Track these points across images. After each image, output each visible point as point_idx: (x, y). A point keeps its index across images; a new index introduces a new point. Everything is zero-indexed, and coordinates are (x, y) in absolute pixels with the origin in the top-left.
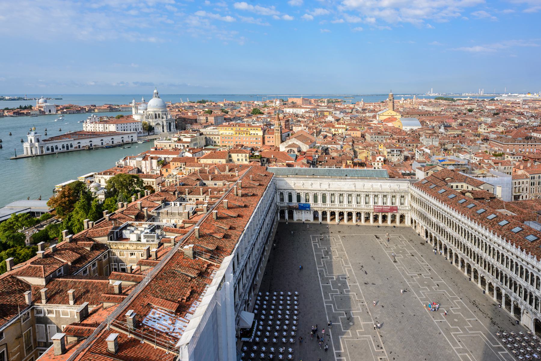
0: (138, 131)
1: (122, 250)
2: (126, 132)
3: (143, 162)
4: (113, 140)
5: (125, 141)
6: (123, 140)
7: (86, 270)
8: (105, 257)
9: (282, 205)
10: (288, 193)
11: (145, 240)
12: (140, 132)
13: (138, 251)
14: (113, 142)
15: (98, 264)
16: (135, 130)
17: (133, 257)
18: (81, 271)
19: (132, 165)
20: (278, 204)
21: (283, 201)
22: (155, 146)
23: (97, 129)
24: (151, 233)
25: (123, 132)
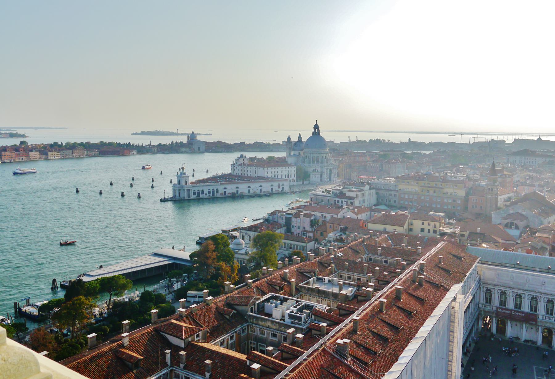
0: (291, 179)
1: (262, 327)
4: (261, 188)
5: (274, 190)
6: (272, 189)
7: (224, 341)
8: (243, 330)
9: (487, 309)
10: (499, 292)
11: (290, 321)
12: (293, 179)
13: (281, 332)
14: (261, 190)
15: (236, 338)
17: (273, 339)
18: (218, 342)
20: (480, 306)
21: (490, 303)
23: (245, 173)
24: (298, 313)
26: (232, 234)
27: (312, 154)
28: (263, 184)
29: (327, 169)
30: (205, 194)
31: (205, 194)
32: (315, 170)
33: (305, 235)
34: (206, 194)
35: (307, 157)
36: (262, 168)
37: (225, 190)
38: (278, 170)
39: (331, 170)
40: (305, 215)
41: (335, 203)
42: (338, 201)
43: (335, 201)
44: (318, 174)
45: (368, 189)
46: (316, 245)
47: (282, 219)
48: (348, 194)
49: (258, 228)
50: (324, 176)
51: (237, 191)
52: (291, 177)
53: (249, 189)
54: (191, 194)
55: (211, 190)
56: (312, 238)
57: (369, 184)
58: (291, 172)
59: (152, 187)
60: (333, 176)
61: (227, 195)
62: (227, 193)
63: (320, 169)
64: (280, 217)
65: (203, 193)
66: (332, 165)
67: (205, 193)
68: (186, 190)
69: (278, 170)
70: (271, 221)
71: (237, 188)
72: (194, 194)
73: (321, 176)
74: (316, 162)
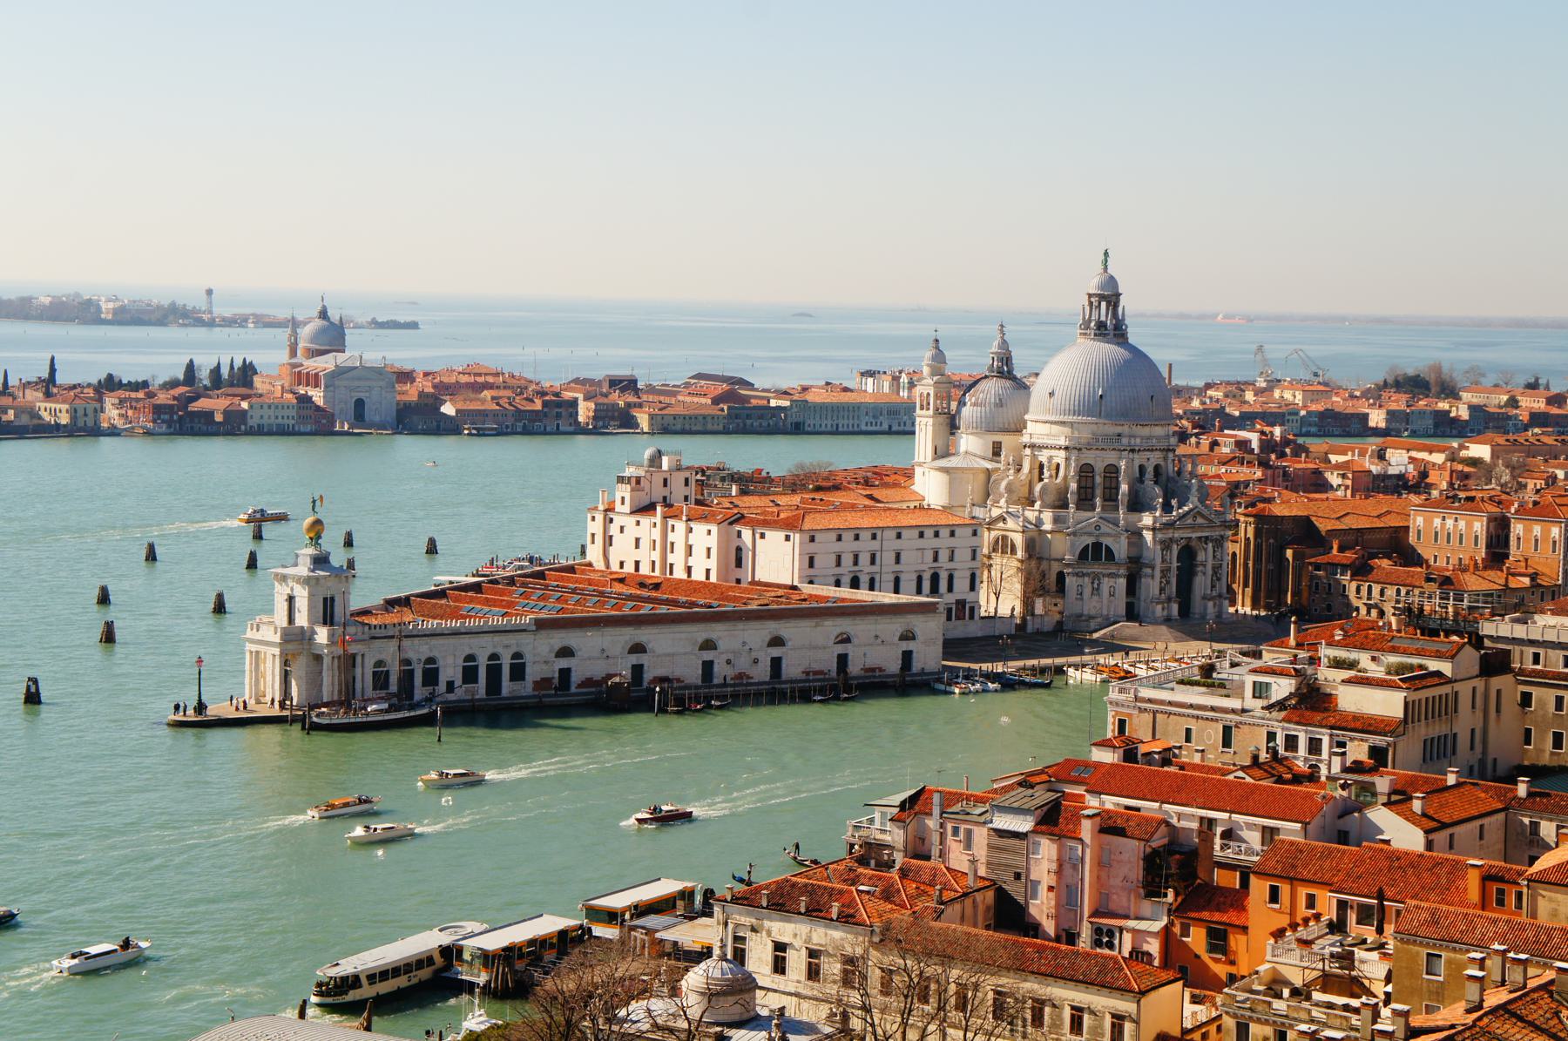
0: (951, 599)
2: (864, 595)
3: (1046, 851)
4: (776, 652)
6: (843, 660)
12: (961, 604)
14: (776, 663)
16: (926, 585)
19: (958, 859)
22: (1110, 732)
23: (677, 558)
25: (845, 592)
26: (650, 932)
27: (1076, 451)
28: (786, 629)
29: (1166, 545)
30: (442, 687)
31: (442, 687)
32: (1097, 546)
33: (1110, 946)
34: (450, 686)
35: (1046, 474)
36: (781, 535)
37: (564, 663)
38: (875, 545)
39: (1188, 555)
40: (1110, 827)
41: (1274, 752)
42: (1291, 742)
43: (1271, 736)
44: (1111, 575)
45: (1476, 670)
46: (1189, 1008)
47: (968, 846)
48: (1352, 700)
49: (832, 893)
50: (1151, 586)
51: (638, 670)
52: (950, 589)
53: (708, 655)
54: (358, 685)
55: (482, 663)
56: (1156, 963)
57: (1477, 641)
58: (951, 559)
59: (109, 637)
60: (1201, 583)
61: (573, 689)
62: (576, 678)
63: (1124, 541)
64: (956, 831)
65: (431, 676)
66: (1200, 520)
67: (443, 678)
68: (327, 661)
69: (875, 545)
70: (899, 858)
71: (638, 648)
72: (381, 679)
73: (1132, 589)
74: (1098, 501)
